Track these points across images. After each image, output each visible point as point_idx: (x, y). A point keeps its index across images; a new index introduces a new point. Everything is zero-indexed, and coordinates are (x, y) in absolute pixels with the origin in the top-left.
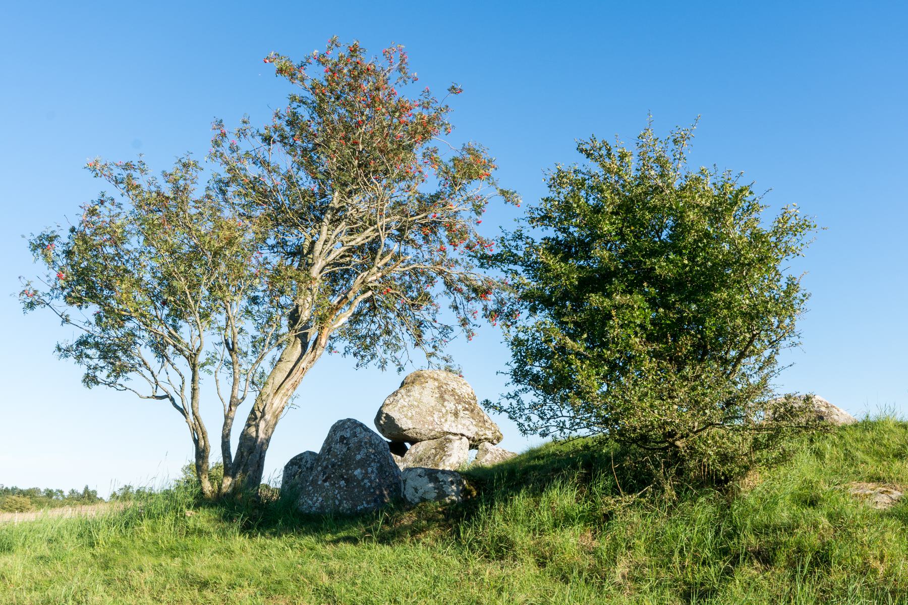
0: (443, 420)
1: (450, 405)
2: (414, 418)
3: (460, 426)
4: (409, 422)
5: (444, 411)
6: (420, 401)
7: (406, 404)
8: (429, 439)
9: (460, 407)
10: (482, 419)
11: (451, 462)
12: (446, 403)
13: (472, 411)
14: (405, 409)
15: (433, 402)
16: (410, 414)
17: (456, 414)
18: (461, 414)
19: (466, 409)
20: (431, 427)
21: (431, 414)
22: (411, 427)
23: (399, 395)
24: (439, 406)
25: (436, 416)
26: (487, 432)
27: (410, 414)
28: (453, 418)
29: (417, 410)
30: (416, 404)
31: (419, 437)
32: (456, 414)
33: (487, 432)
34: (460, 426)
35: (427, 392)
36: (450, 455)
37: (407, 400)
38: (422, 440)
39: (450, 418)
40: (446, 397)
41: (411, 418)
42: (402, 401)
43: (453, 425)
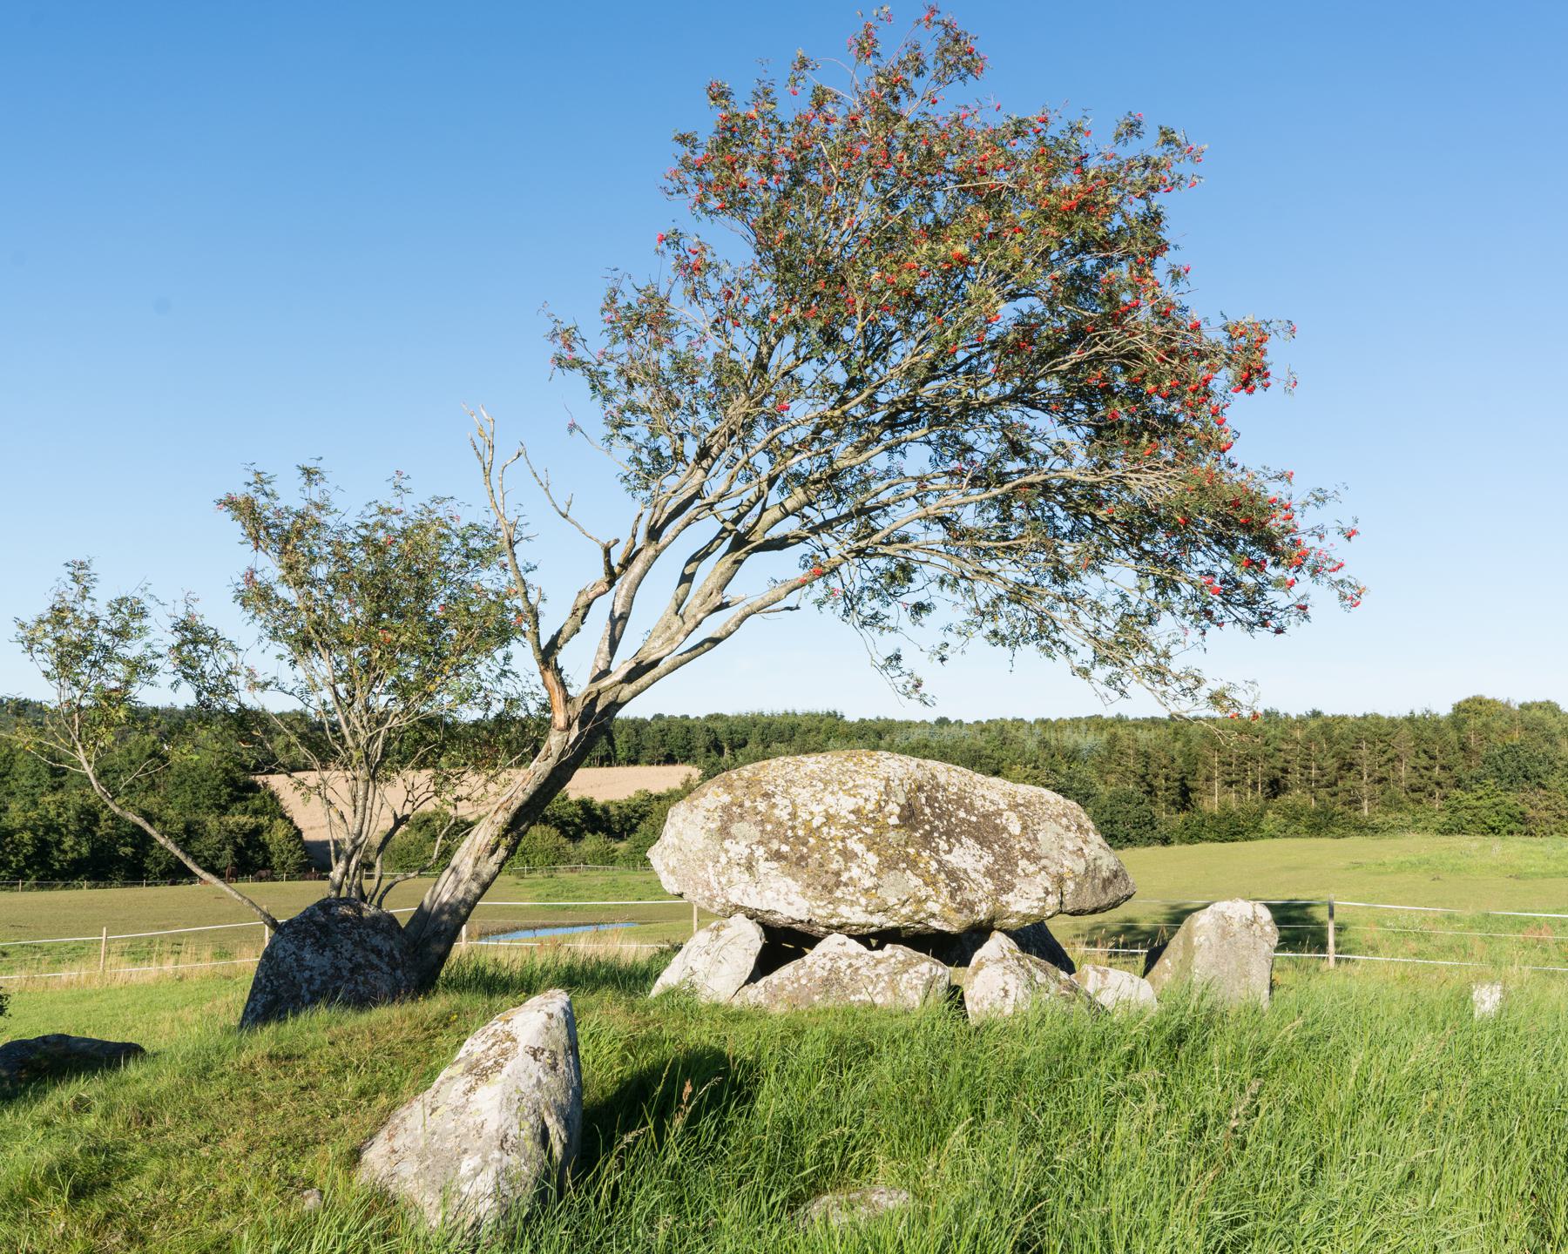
0: (724, 880)
1: (738, 849)
3: (769, 894)
4: (672, 879)
5: (723, 860)
12: (727, 844)
17: (750, 868)
18: (762, 866)
19: (778, 856)
20: (707, 894)
26: (844, 910)
28: (746, 877)
32: (750, 868)
33: (844, 910)
35: (699, 815)
40: (734, 829)
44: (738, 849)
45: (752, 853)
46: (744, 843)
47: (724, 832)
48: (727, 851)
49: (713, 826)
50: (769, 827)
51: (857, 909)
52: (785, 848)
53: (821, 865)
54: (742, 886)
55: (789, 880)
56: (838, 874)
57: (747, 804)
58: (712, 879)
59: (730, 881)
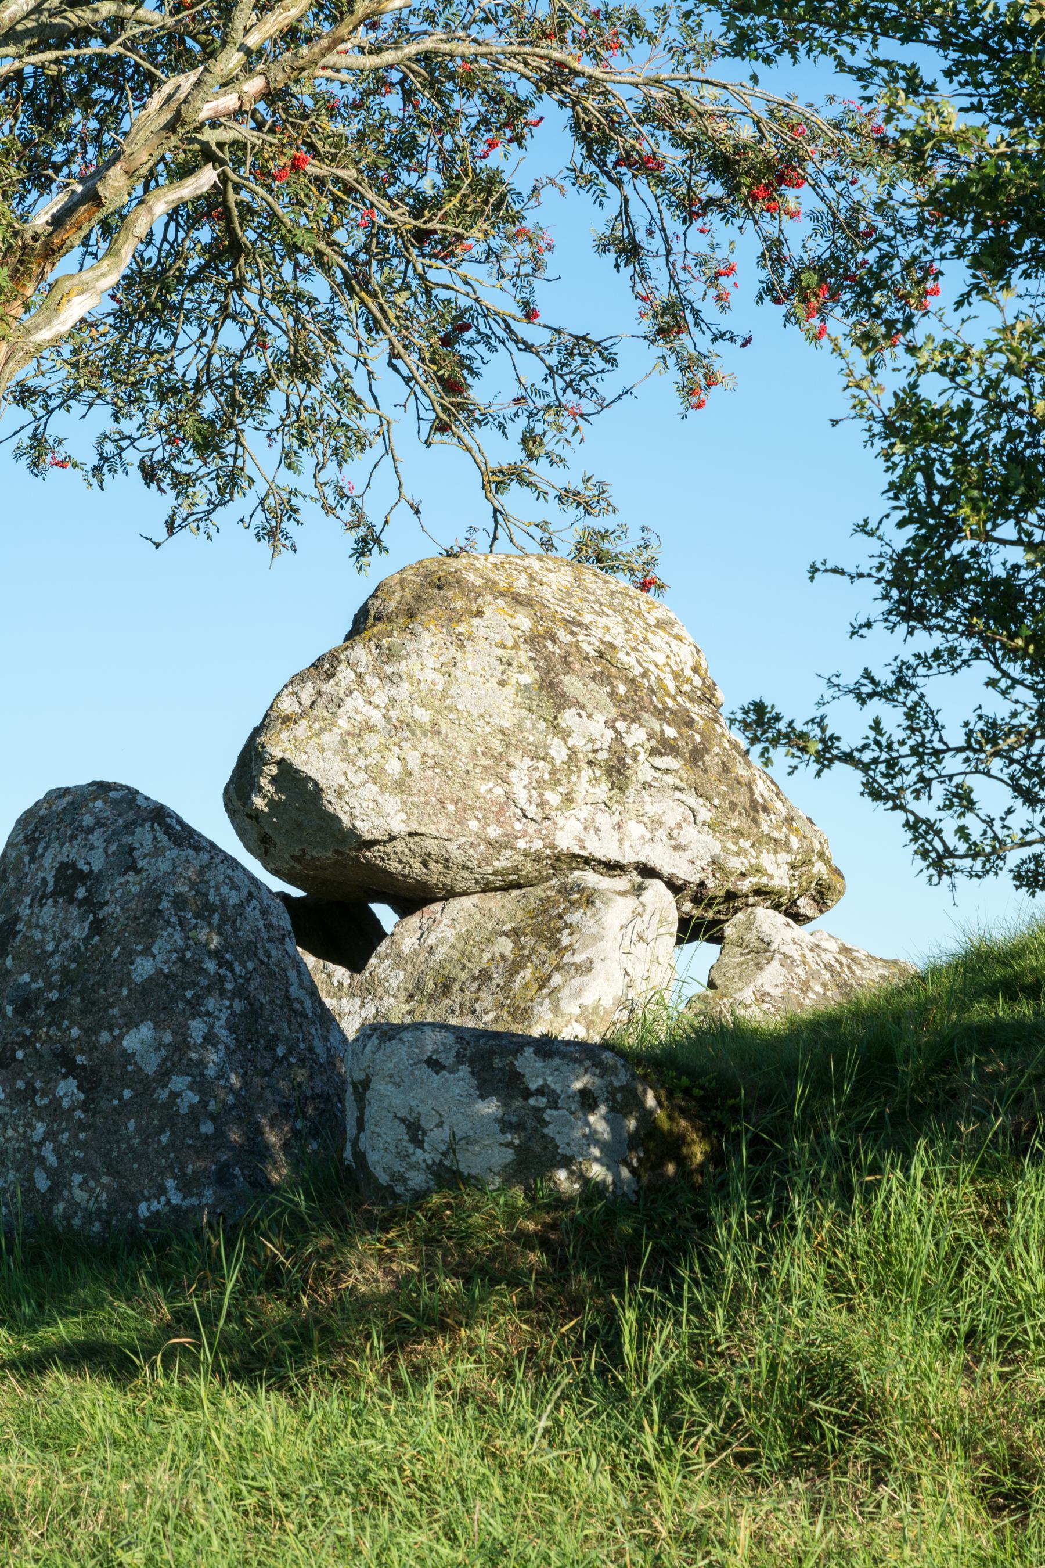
0: (553, 798)
1: (590, 728)
2: (416, 784)
3: (635, 829)
4: (391, 803)
5: (559, 752)
6: (442, 703)
7: (376, 717)
8: (488, 888)
9: (636, 736)
10: (742, 798)
11: (588, 999)
12: (569, 717)
13: (697, 755)
14: (372, 741)
15: (505, 708)
16: (394, 767)
17: (617, 771)
18: (643, 770)
19: (665, 747)
20: (494, 832)
21: (499, 767)
22: (398, 827)
23: (345, 674)
24: (535, 731)
25: (519, 779)
26: (767, 860)
27: (394, 767)
28: (602, 791)
29: (432, 746)
30: (423, 715)
31: (435, 875)
32: (617, 771)
33: (767, 860)
34: (635, 829)
35: (478, 660)
36: (585, 968)
37: (381, 698)
38: (450, 894)
39: (591, 787)
40: (571, 685)
41: (399, 786)
42: (357, 700)
43: (604, 820)
44: (590, 728)
45: (618, 738)
46: (600, 717)
47: (550, 694)
48: (565, 734)
49: (526, 679)
50: (622, 689)
51: (784, 857)
52: (670, 732)
53: (726, 770)
54: (584, 812)
55: (691, 799)
56: (749, 785)
57: (563, 636)
58: (522, 796)
59: (568, 799)
